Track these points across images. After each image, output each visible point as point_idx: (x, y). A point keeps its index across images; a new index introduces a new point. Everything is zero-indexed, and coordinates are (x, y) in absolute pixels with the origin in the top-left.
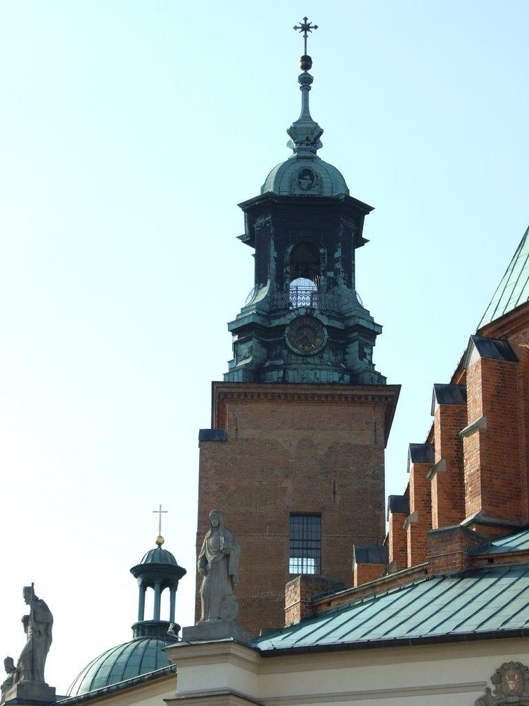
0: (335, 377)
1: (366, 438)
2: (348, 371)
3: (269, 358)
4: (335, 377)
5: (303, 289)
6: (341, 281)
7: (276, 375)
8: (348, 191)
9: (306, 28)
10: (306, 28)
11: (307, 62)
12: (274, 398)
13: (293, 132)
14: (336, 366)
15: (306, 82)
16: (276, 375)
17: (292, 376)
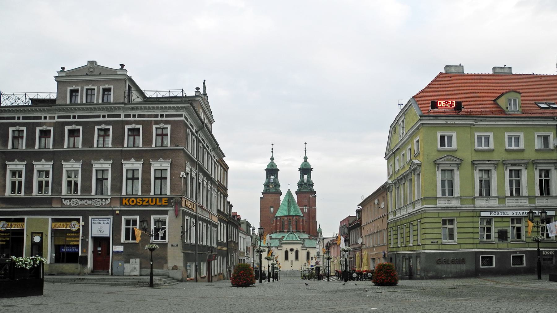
0: (275, 191)
1: (278, 198)
2: (277, 190)
3: (268, 188)
4: (275, 191)
5: (272, 177)
6: (276, 179)
7: (268, 191)
8: (277, 166)
9: (272, 144)
10: (272, 144)
11: (272, 149)
12: (268, 194)
13: (271, 159)
14: (275, 189)
15: (272, 151)
16: (268, 191)
17: (270, 191)
